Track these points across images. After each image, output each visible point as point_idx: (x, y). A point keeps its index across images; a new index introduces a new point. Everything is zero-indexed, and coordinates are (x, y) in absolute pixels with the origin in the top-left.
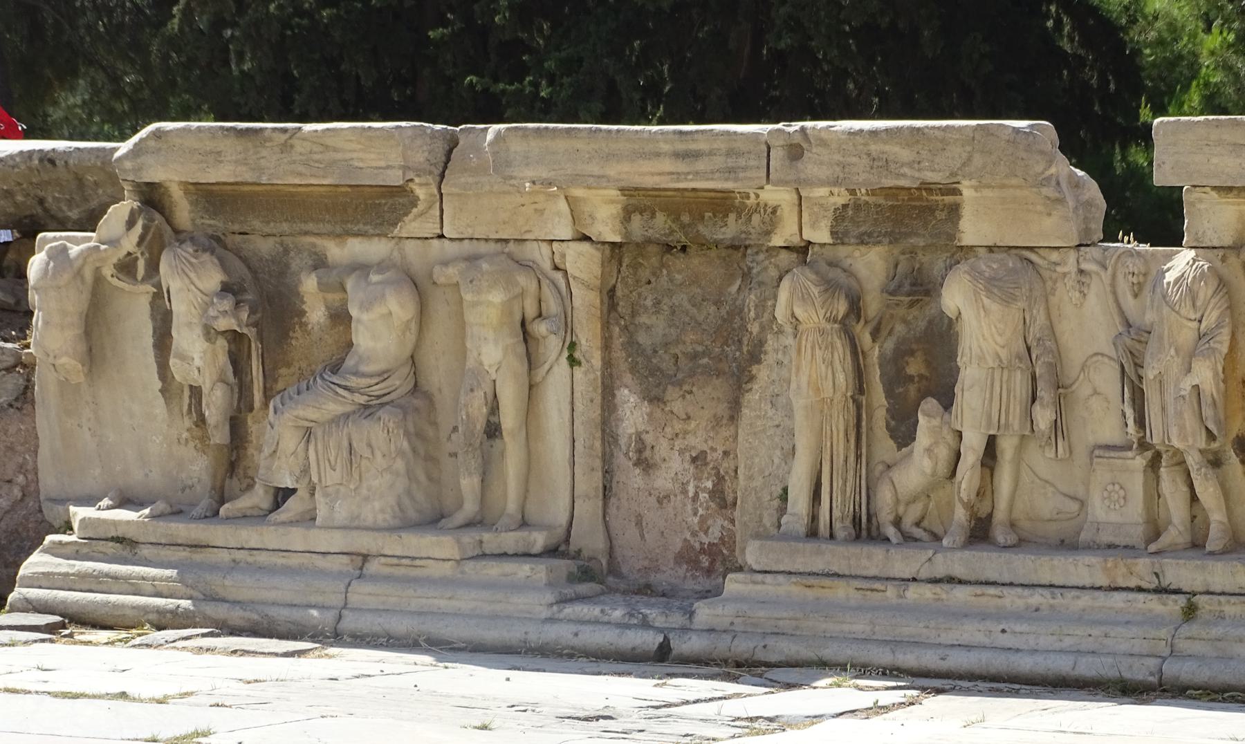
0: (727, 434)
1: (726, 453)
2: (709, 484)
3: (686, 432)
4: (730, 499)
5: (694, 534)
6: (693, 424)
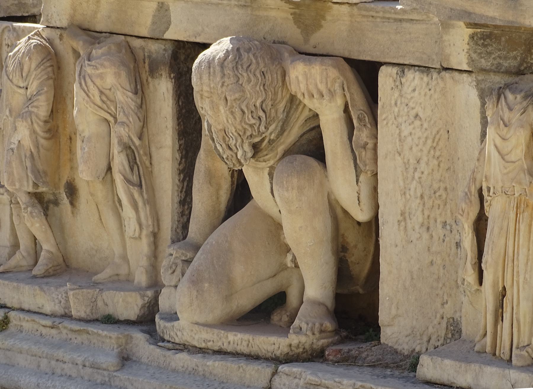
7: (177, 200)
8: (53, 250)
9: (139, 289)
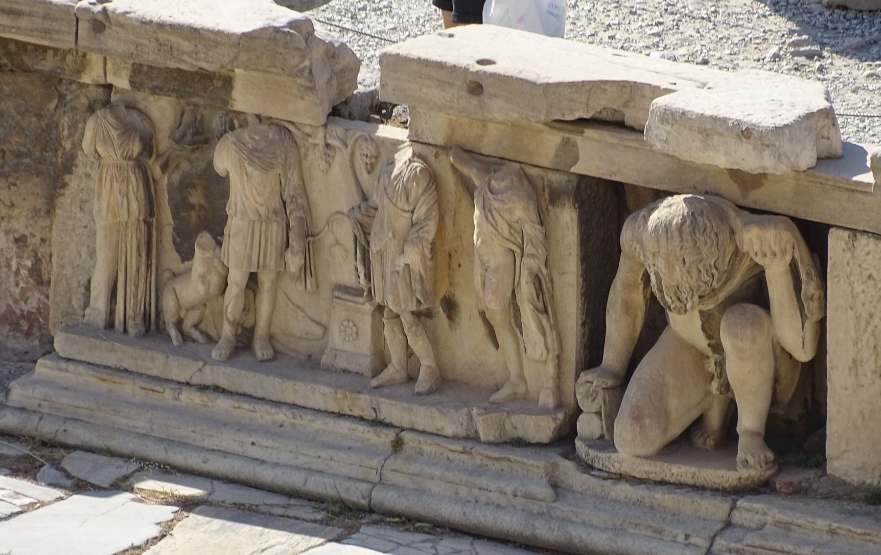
0: (44, 224)
1: (43, 240)
2: (29, 263)
3: (10, 217)
4: (45, 278)
5: (16, 302)
6: (16, 212)
7: (580, 322)
8: (433, 365)
9: (545, 411)
